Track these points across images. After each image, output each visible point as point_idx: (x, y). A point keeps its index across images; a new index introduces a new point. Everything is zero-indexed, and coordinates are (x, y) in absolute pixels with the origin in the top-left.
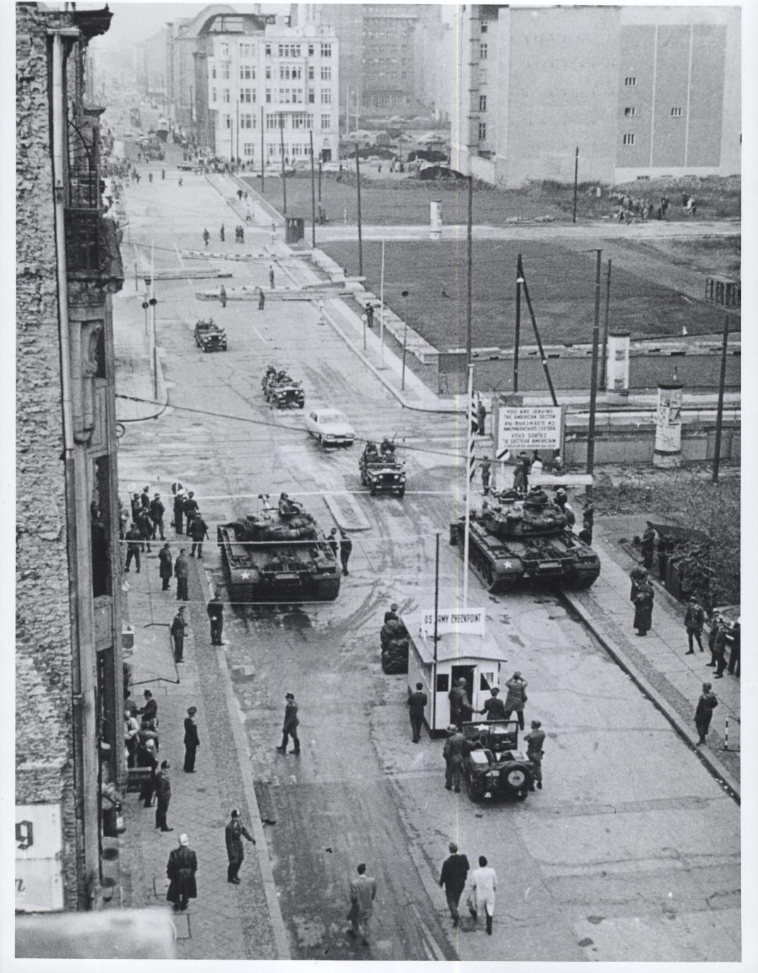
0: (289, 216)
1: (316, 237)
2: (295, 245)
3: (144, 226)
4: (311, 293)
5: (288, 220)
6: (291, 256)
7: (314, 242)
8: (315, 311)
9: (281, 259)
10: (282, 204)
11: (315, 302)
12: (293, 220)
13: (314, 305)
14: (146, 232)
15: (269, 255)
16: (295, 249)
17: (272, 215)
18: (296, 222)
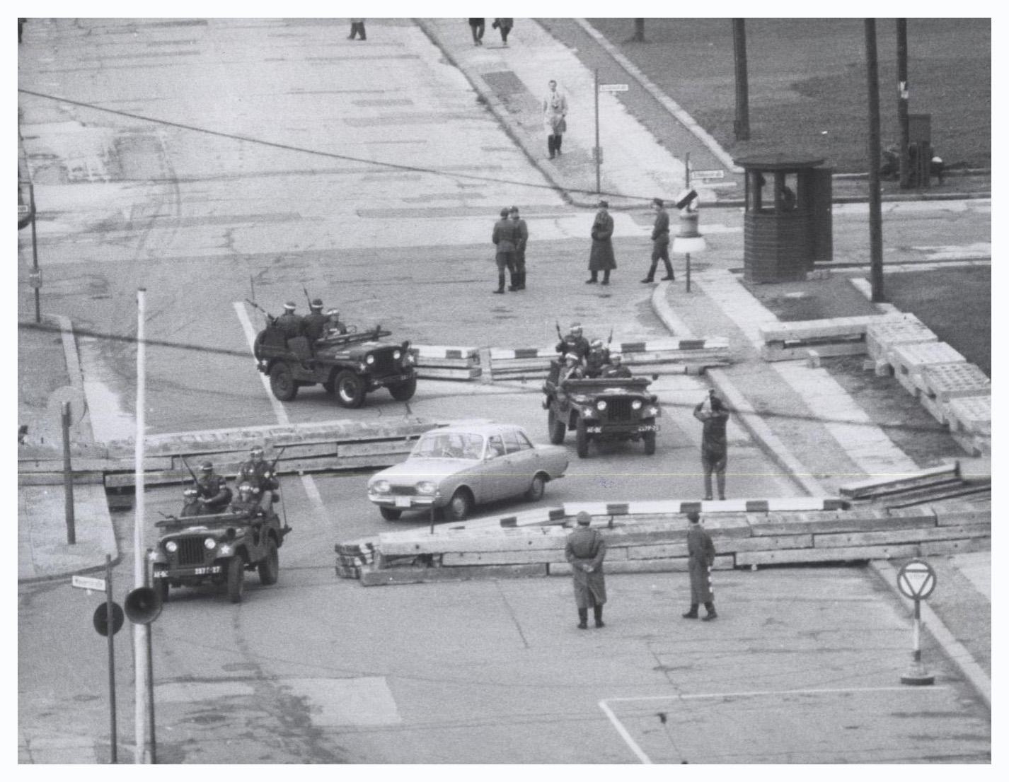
0: (764, 154)
1: (888, 251)
2: (795, 292)
3: (104, 227)
4: (867, 526)
5: (755, 173)
6: (772, 343)
7: (877, 277)
8: (886, 613)
9: (728, 363)
10: (728, 100)
11: (890, 574)
12: (781, 172)
13: (881, 587)
14: (107, 253)
15: (674, 344)
16: (790, 311)
17: (685, 150)
18: (791, 182)
